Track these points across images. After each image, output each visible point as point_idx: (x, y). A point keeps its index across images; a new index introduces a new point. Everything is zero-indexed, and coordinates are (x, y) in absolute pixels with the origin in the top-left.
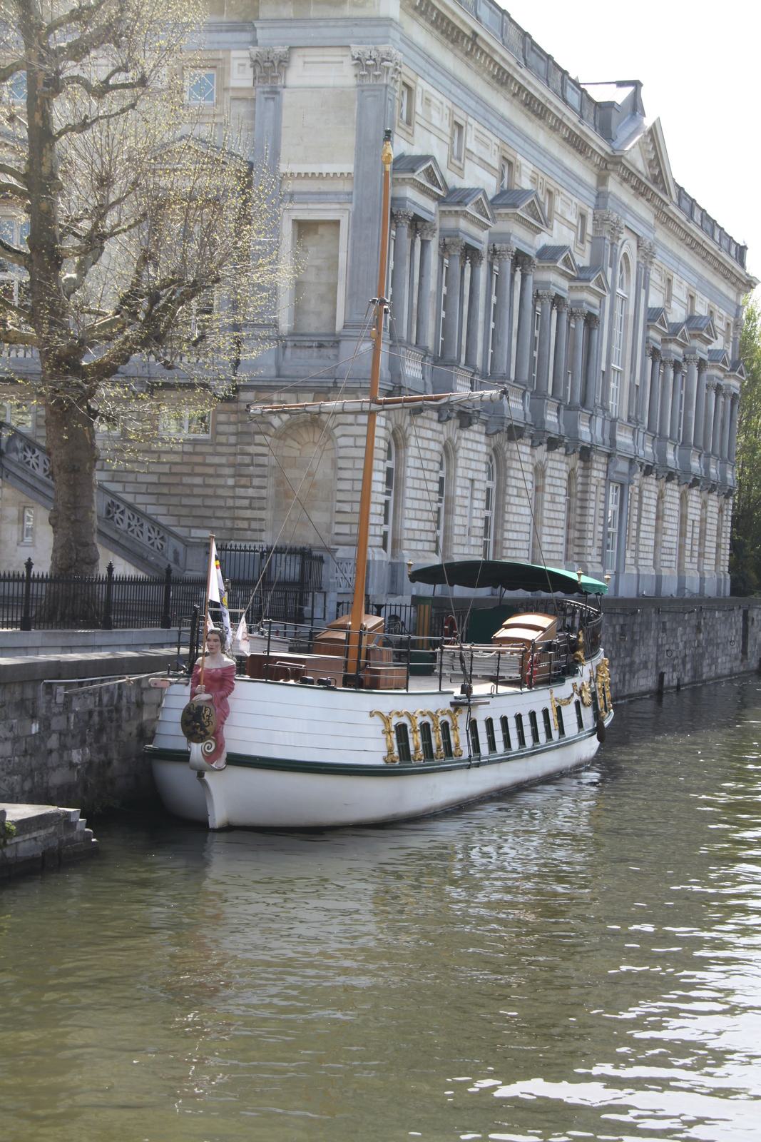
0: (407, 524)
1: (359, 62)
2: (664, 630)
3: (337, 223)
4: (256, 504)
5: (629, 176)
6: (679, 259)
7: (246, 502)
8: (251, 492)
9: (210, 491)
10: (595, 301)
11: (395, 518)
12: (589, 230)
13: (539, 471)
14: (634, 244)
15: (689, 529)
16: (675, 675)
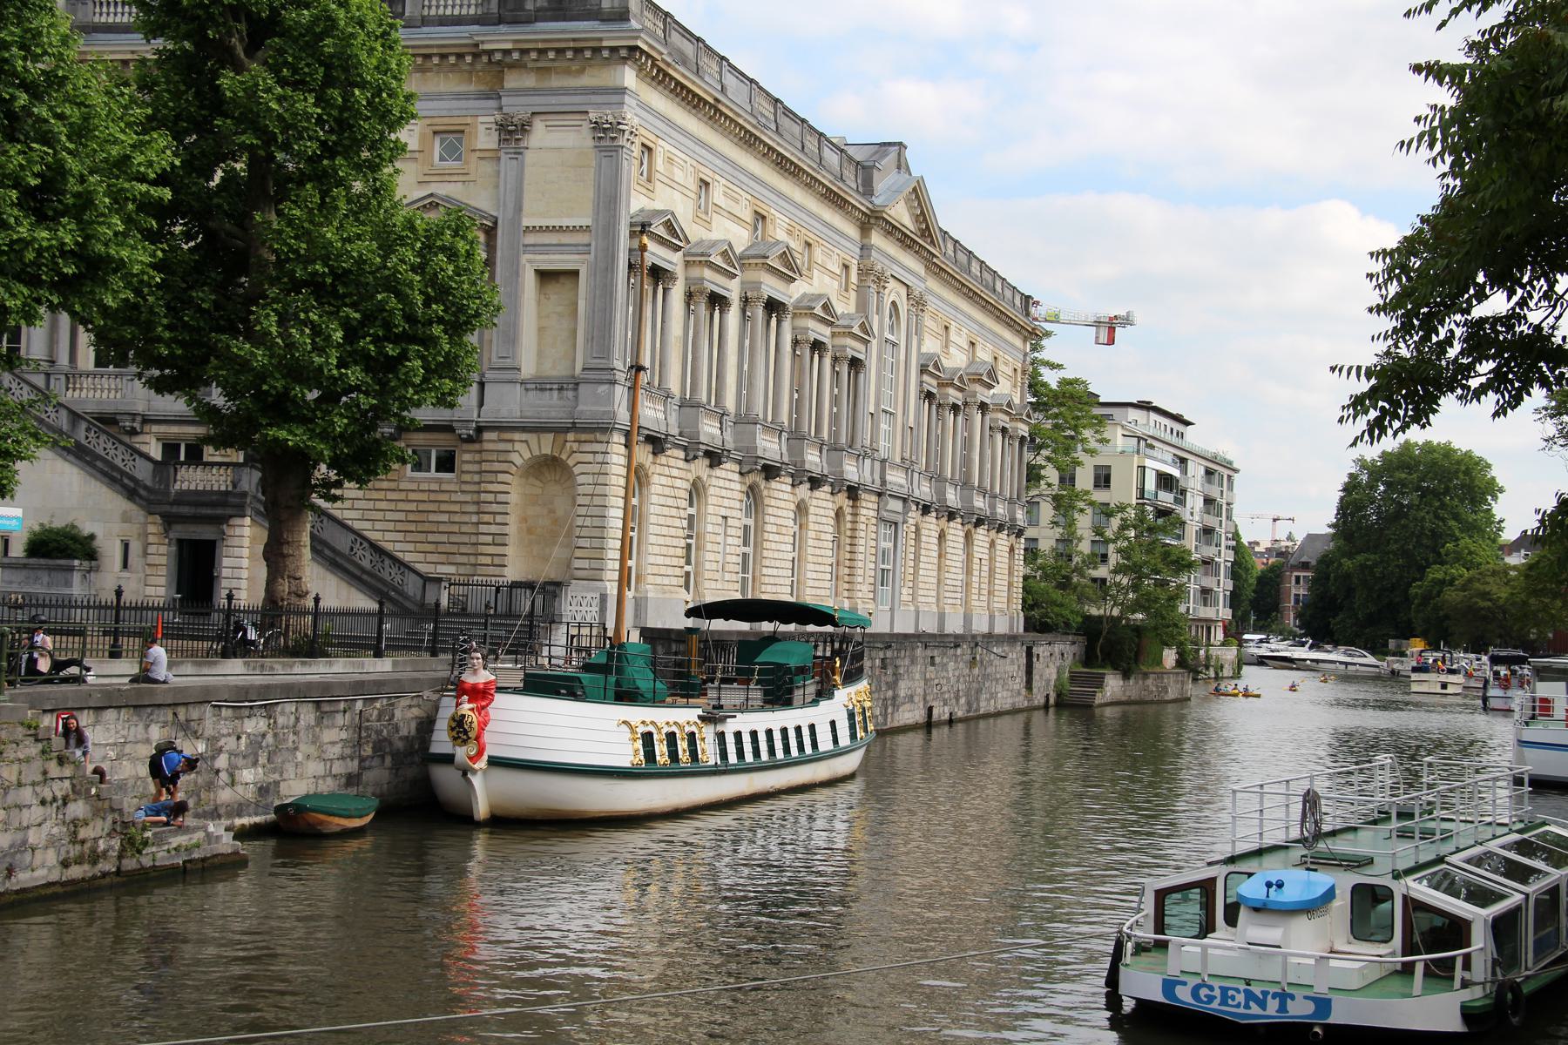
0: (651, 559)
1: (597, 126)
2: (933, 664)
3: (575, 274)
5: (892, 230)
6: (956, 308)
7: (489, 539)
8: (493, 529)
9: (455, 528)
10: (861, 347)
11: (638, 553)
12: (854, 278)
13: (801, 509)
14: (903, 291)
15: (976, 567)
16: (947, 709)
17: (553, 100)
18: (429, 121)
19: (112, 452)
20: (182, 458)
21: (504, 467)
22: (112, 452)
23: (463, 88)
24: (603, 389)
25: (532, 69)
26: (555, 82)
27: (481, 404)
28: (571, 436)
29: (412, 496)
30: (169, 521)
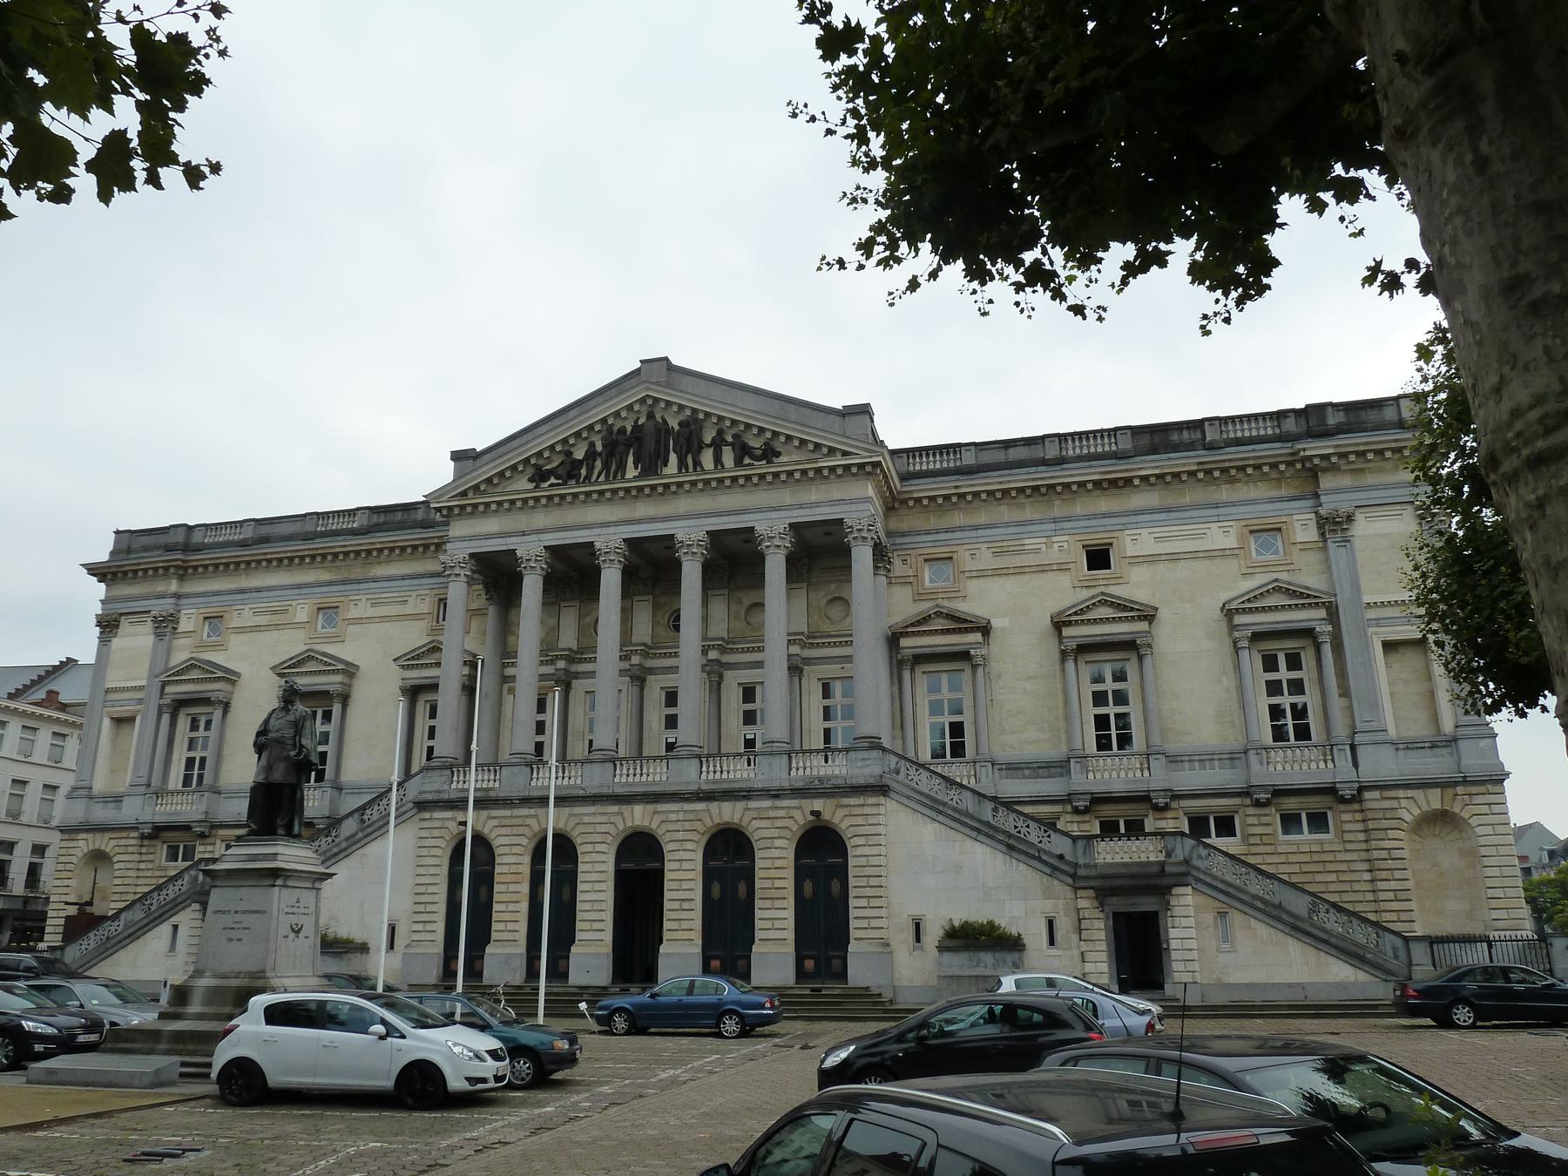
4: (1401, 895)
7: (1391, 895)
8: (1393, 885)
9: (1347, 887)
17: (1374, 494)
19: (1024, 830)
20: (1122, 830)
21: (1393, 823)
22: (1024, 830)
23: (1274, 493)
24: (1483, 743)
25: (1346, 471)
26: (1370, 479)
27: (1356, 764)
28: (1460, 790)
29: (1293, 858)
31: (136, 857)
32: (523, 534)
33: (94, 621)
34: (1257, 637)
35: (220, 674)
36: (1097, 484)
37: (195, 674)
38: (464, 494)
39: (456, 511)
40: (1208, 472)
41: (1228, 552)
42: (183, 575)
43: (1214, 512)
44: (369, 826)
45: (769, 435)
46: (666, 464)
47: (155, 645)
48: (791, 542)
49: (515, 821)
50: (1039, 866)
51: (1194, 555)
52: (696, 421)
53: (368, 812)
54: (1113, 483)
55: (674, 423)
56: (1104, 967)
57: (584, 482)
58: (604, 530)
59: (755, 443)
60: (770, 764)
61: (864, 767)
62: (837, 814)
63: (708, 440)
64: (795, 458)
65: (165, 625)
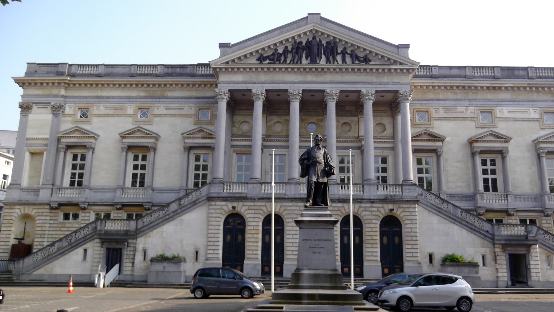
18: (542, 109)
22: (473, 220)
30: (504, 247)
31: (49, 218)
32: (255, 83)
33: (18, 106)
34: (482, 152)
35: (92, 135)
36: (488, 88)
37: (138, 134)
38: (227, 63)
39: (224, 70)
40: (531, 88)
41: (536, 120)
42: (66, 87)
43: (531, 103)
44: (183, 207)
45: (368, 52)
46: (320, 59)
47: (53, 119)
48: (229, 97)
49: (255, 208)
50: (479, 235)
51: (523, 119)
52: (335, 43)
53: (183, 201)
54: (494, 88)
55: (324, 42)
56: (506, 274)
57: (282, 63)
58: (293, 85)
59: (361, 55)
60: (370, 189)
61: (410, 192)
62: (400, 212)
63: (339, 51)
64: (377, 63)
65: (57, 110)
